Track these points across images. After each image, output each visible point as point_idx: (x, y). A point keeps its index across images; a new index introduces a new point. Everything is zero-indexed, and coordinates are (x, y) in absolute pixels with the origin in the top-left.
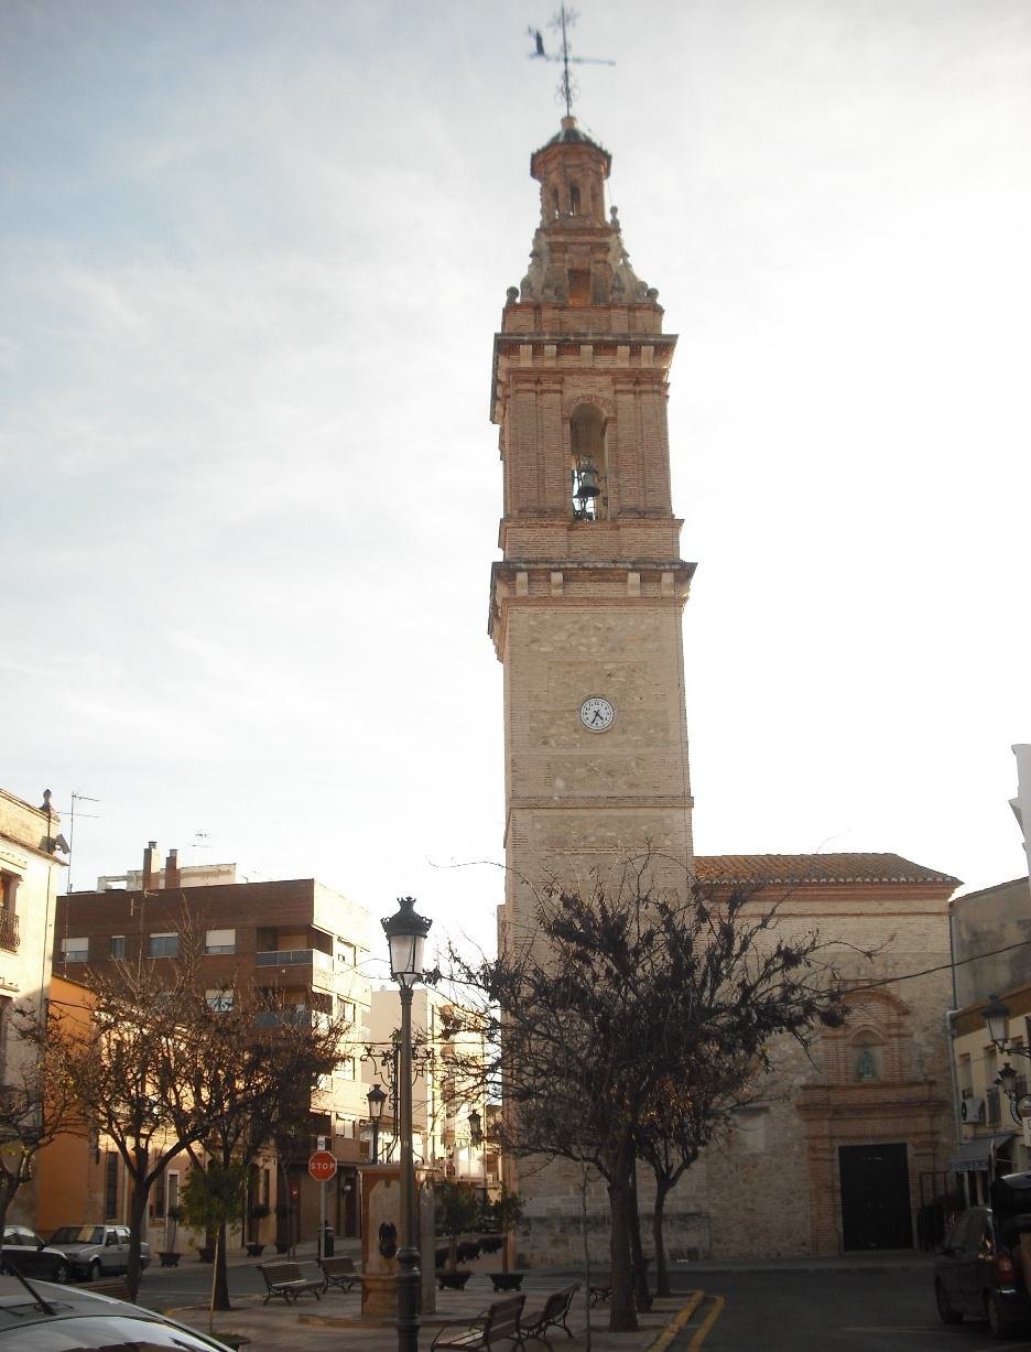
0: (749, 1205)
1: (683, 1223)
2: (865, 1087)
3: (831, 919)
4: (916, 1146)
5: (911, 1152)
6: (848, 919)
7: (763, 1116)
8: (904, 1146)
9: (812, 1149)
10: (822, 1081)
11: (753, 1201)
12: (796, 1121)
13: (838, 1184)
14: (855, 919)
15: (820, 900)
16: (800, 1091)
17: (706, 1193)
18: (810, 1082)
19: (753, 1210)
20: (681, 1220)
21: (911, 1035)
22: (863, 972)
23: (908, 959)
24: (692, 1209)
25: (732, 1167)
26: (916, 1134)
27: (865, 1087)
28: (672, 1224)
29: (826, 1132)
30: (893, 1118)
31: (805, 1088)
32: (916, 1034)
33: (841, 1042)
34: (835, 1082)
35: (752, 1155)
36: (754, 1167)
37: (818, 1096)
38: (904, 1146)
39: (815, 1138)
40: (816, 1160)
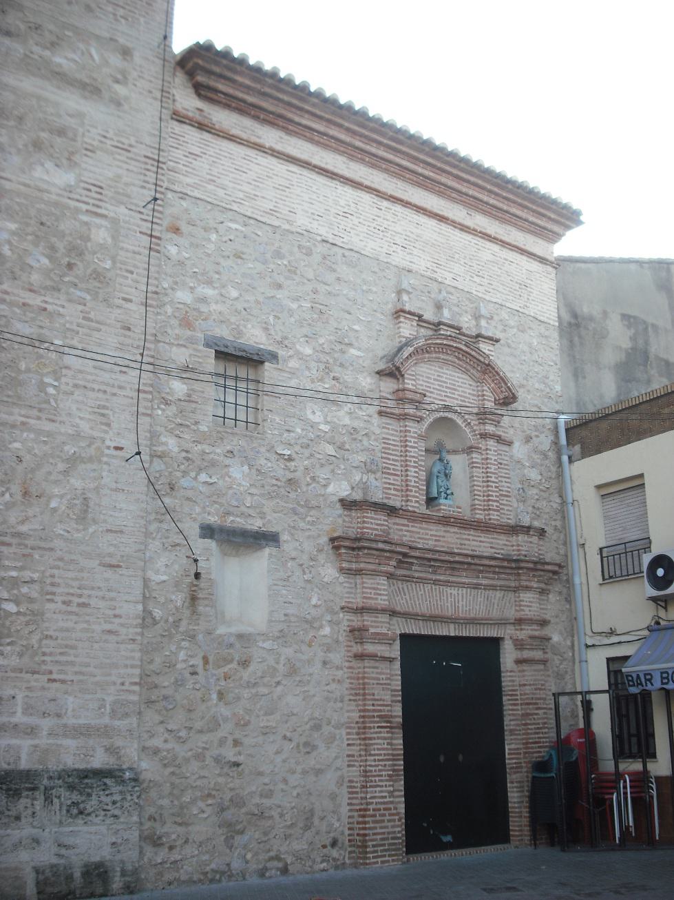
0: (230, 754)
1: (75, 797)
2: (445, 521)
3: (398, 208)
4: (519, 644)
5: (508, 656)
6: (423, 219)
7: (267, 551)
8: (496, 642)
9: (357, 633)
10: (378, 497)
11: (236, 743)
12: (329, 571)
13: (398, 710)
14: (432, 223)
15: (386, 171)
16: (339, 510)
17: (134, 720)
18: (358, 496)
19: (237, 765)
20: (71, 787)
21: (510, 444)
22: (446, 313)
23: (504, 315)
24: (99, 760)
25: (198, 661)
26: (519, 622)
27: (445, 521)
28: (48, 800)
29: (382, 602)
30: (487, 587)
31: (348, 504)
32: (516, 444)
33: (413, 427)
34: (397, 503)
35: (240, 636)
36: (245, 663)
37: (375, 523)
38: (496, 642)
39: (361, 610)
40: (360, 657)
